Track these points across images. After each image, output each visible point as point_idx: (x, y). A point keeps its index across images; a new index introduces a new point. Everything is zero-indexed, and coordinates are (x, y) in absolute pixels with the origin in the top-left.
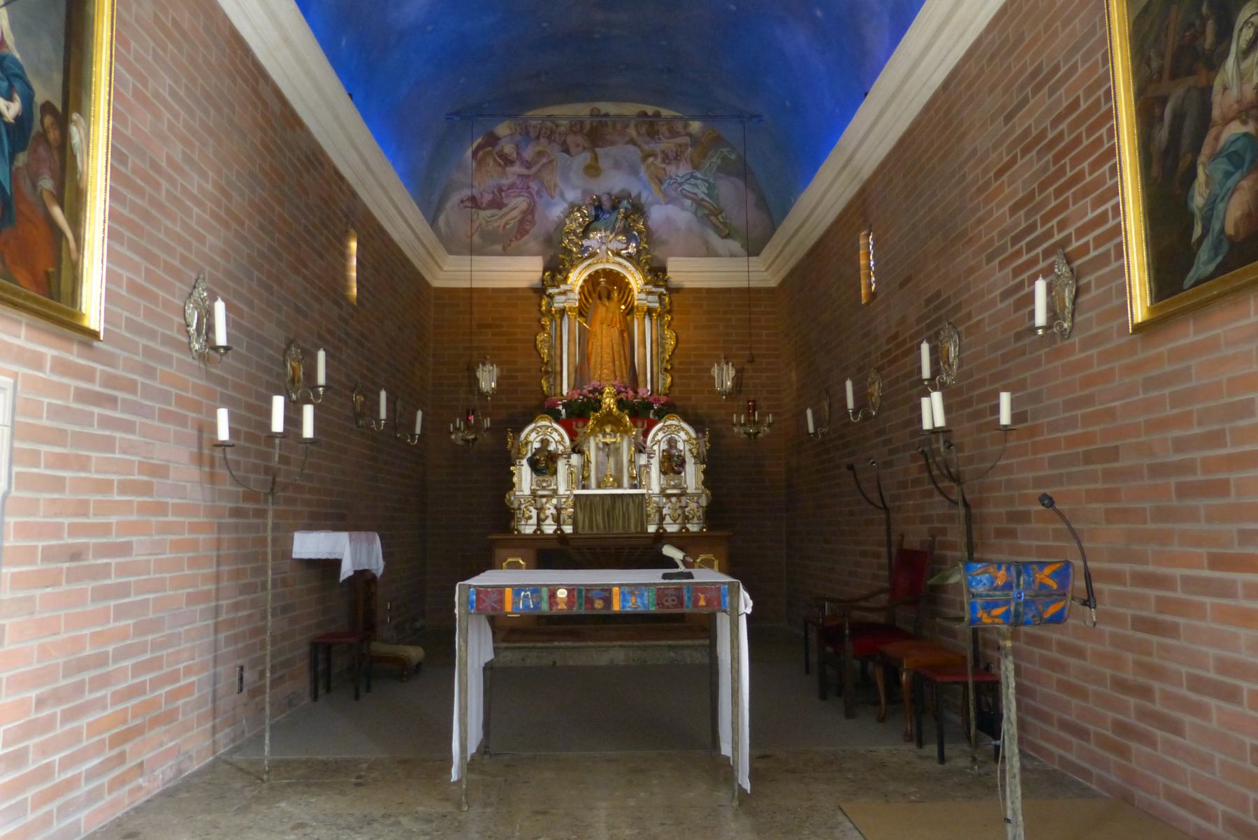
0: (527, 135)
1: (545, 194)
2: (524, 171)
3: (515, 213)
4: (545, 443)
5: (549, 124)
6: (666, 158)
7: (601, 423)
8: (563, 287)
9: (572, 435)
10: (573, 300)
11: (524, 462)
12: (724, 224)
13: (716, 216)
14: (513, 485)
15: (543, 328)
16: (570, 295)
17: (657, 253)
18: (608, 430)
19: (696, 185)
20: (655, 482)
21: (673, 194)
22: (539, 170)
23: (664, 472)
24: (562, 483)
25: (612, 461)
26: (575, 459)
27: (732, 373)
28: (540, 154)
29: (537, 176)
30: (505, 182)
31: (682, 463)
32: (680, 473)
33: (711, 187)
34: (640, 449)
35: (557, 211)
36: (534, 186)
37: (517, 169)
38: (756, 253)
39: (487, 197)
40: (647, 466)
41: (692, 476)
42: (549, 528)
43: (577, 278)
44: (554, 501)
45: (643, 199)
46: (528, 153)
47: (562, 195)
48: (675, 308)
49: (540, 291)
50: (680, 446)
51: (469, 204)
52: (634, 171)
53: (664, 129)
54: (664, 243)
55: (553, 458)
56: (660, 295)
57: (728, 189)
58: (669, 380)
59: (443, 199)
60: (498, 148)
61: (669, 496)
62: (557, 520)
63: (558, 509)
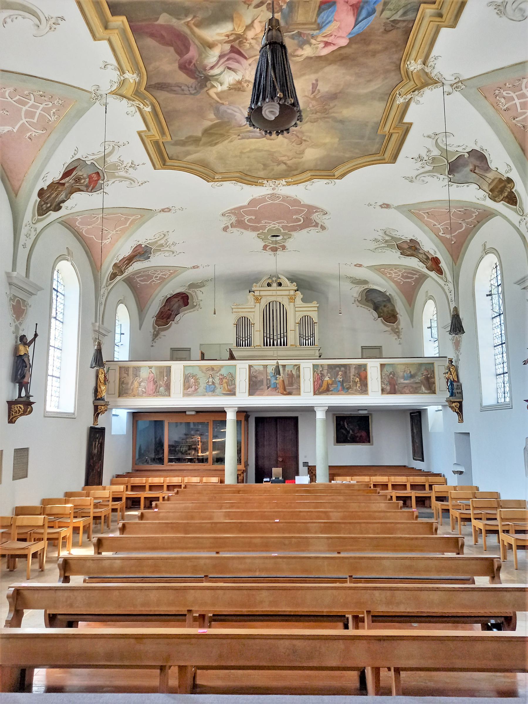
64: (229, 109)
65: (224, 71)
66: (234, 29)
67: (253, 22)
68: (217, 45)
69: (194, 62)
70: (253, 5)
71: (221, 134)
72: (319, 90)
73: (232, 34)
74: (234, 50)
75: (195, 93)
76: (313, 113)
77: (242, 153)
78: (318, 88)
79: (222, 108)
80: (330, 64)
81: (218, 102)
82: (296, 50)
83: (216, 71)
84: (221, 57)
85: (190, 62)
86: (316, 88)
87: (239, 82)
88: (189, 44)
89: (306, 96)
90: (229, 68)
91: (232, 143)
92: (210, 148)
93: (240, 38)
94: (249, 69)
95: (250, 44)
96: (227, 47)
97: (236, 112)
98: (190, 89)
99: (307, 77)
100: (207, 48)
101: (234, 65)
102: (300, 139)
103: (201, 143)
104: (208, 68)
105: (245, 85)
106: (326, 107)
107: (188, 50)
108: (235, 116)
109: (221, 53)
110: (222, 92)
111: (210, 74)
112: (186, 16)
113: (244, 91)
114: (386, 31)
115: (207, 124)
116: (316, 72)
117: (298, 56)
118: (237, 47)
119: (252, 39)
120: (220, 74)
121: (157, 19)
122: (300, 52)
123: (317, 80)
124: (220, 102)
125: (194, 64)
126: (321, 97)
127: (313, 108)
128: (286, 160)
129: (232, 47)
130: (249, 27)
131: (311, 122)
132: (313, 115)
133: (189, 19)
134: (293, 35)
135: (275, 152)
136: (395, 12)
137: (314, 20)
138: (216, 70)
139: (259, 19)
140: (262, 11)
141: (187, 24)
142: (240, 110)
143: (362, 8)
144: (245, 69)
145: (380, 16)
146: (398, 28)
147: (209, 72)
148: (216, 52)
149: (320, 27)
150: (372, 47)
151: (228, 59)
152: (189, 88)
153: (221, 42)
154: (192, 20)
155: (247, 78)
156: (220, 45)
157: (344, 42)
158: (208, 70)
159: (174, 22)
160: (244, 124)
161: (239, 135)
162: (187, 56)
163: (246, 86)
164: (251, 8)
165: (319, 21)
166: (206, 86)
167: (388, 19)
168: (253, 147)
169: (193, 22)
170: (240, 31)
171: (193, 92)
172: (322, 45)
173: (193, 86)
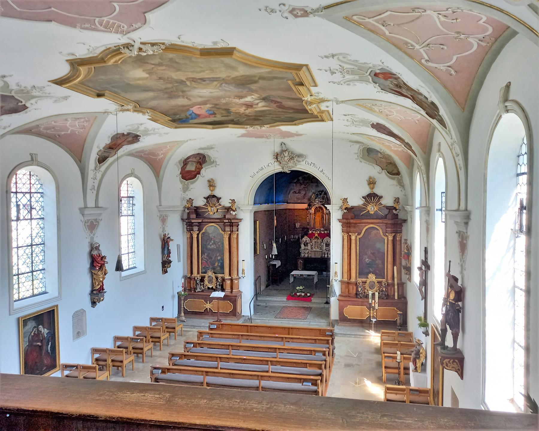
9: (311, 240)
29: (307, 187)
35: (310, 194)
36: (306, 189)
42: (306, 255)
49: (307, 209)
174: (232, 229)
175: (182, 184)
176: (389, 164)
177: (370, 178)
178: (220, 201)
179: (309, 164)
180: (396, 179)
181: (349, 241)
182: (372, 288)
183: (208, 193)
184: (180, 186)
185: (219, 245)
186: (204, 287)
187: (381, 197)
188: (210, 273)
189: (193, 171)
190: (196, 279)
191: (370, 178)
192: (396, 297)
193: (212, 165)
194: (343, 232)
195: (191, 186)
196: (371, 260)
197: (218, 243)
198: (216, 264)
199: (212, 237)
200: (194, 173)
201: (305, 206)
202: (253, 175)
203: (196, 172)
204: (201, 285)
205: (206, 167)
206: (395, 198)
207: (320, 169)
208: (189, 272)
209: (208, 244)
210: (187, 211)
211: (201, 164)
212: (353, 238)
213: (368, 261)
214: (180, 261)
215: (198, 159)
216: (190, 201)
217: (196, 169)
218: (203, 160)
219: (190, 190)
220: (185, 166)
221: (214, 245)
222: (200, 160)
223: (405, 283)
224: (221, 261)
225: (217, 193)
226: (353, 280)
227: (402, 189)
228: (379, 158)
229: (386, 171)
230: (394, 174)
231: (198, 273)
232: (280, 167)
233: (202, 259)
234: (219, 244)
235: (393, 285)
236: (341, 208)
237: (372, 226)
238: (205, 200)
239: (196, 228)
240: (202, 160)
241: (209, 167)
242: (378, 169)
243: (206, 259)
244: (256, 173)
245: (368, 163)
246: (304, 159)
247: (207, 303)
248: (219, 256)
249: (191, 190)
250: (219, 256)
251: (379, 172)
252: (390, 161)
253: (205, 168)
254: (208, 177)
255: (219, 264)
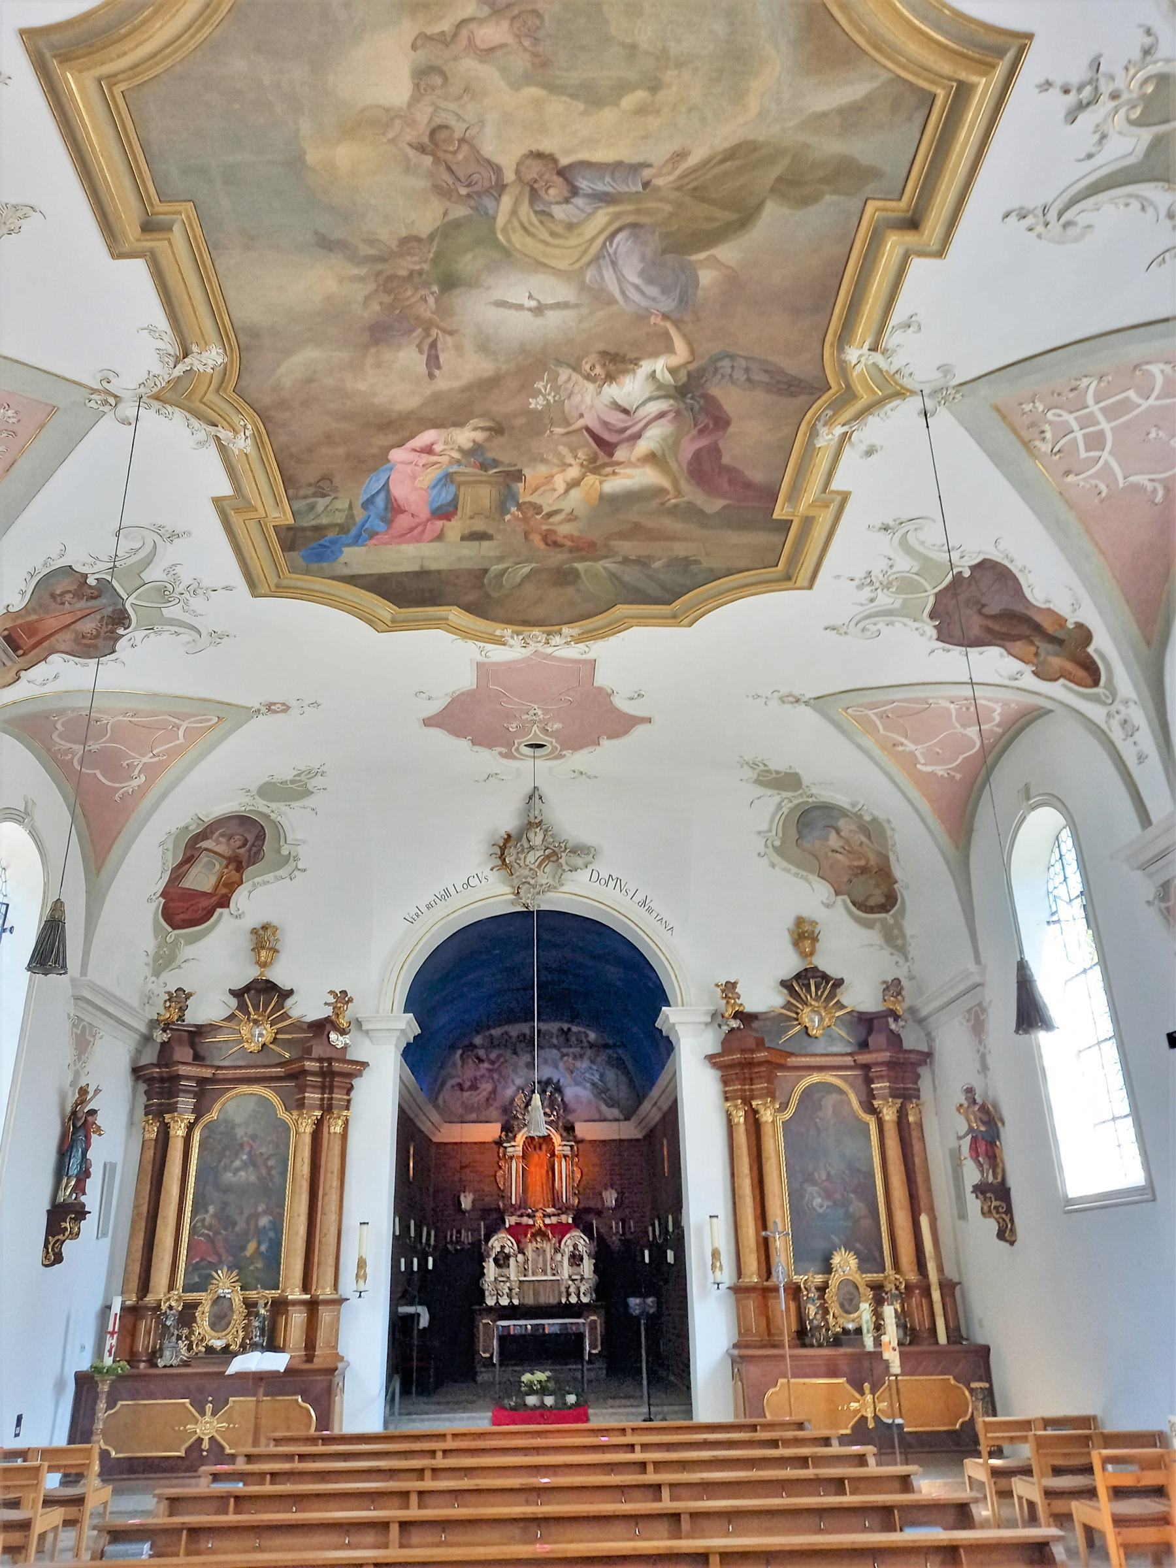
0: (492, 1044)
1: (502, 1080)
2: (490, 1066)
3: (484, 1093)
4: (503, 1247)
5: (506, 1037)
6: (575, 1058)
7: (534, 1235)
8: (513, 1144)
9: (518, 1242)
10: (519, 1151)
11: (491, 1260)
12: (610, 1098)
13: (605, 1093)
14: (484, 1274)
15: (500, 1167)
16: (517, 1148)
17: (570, 1118)
18: (539, 1239)
19: (593, 1074)
20: (566, 1270)
21: (580, 1080)
22: (500, 1066)
23: (571, 1265)
24: (513, 1272)
25: (541, 1259)
26: (520, 1257)
27: (615, 1195)
28: (499, 1056)
30: (478, 1074)
31: (581, 1259)
32: (579, 1265)
33: (602, 1076)
34: (557, 1250)
35: (510, 1092)
37: (486, 1065)
38: (627, 1119)
39: (467, 1084)
40: (561, 1262)
41: (587, 1266)
43: (520, 1138)
44: (508, 1284)
45: (561, 1084)
46: (493, 1056)
47: (513, 1082)
48: (580, 1153)
49: (499, 1143)
50: (580, 1248)
51: (456, 1088)
52: (556, 1067)
53: (573, 1039)
54: (574, 1111)
55: (507, 1257)
56: (571, 1146)
57: (611, 1075)
58: (577, 1201)
59: (443, 1085)
60: (475, 1052)
61: (573, 1280)
62: (510, 1296)
63: (510, 1289)
64: (654, 300)
65: (637, 408)
66: (601, 483)
67: (567, 491)
68: (638, 460)
69: (694, 432)
70: (564, 513)
71: (703, 200)
72: (421, 352)
73: (607, 475)
74: (607, 447)
75: (720, 359)
76: (420, 273)
77: (654, 86)
78: (425, 357)
79: (668, 304)
80: (412, 412)
81: (677, 324)
82: (488, 440)
83: (654, 407)
84: (638, 436)
85: (701, 432)
86: (428, 356)
87: (610, 378)
88: (690, 464)
89: (451, 333)
90: (626, 411)
91: (675, 146)
92: (761, 134)
93: (593, 466)
94: (583, 407)
95: (576, 457)
96: (620, 454)
97: (637, 287)
98: (729, 370)
99: (457, 384)
100: (659, 453)
101: (616, 419)
102: (441, 154)
103: (775, 172)
104: (672, 415)
105: (598, 370)
106: (387, 299)
107: (697, 457)
108: (642, 273)
109: (634, 444)
110: (655, 355)
111: (672, 402)
112: (676, 506)
113: (604, 354)
114: (327, 478)
115: (728, 252)
116: (437, 397)
117: (483, 429)
118: (601, 454)
119: (571, 465)
120: (650, 399)
121: (725, 507)
122: (480, 436)
123: (431, 376)
124: (669, 325)
125: (695, 425)
126: (410, 331)
127: (422, 292)
128: (481, 21)
129: (611, 455)
130: (574, 484)
131: (418, 239)
132: (417, 267)
133: (673, 501)
134: (495, 467)
135: (527, 79)
136: (330, 508)
137: (462, 488)
138: (654, 409)
139: (556, 494)
140: (550, 505)
141: (679, 493)
142: (623, 293)
143: (386, 508)
144: (592, 407)
145: (351, 502)
146: (310, 485)
147: (671, 405)
148: (644, 446)
149: (448, 478)
150: (341, 451)
151: (624, 430)
152: (731, 376)
153: (629, 464)
154: (669, 500)
155: (591, 387)
156: (633, 459)
157: (396, 455)
158: (670, 411)
159: (700, 499)
160: (620, 237)
161: (646, 185)
162: (704, 442)
163: (598, 367)
164: (568, 510)
165: (453, 489)
166: (689, 374)
167: (336, 498)
168: (608, 115)
169: (669, 497)
170: (591, 479)
171: (726, 363)
172: (438, 448)
173: (719, 376)
174: (331, 1099)
175: (156, 937)
176: (856, 875)
177: (800, 921)
178: (289, 1002)
179: (603, 882)
180: (878, 926)
181: (752, 1129)
182: (850, 1309)
183: (247, 974)
184: (149, 943)
185: (270, 1169)
186: (190, 1348)
187: (839, 983)
188: (225, 1284)
189: (204, 894)
190: (164, 1307)
191: (800, 921)
192: (942, 1338)
193: (280, 873)
194: (727, 1099)
195: (188, 951)
196: (830, 1203)
197: (268, 1159)
198: (251, 1247)
199: (245, 1139)
200: (205, 903)
201: (490, 1131)
202: (412, 913)
203: (213, 900)
204: (179, 1338)
205: (256, 880)
206: (885, 982)
207: (639, 897)
208: (134, 1284)
209: (226, 1168)
210: (160, 1036)
211: (240, 869)
212: (767, 1116)
213: (821, 1206)
214: (105, 1235)
215: (238, 843)
216: (179, 998)
217: (217, 887)
218: (254, 849)
219: (179, 967)
220: (187, 866)
221: (251, 1169)
222: (242, 851)
223: (959, 1283)
224: (271, 1234)
225: (280, 975)
226: (780, 1277)
227: (895, 958)
228: (830, 854)
229: (846, 897)
230: (871, 910)
231: (171, 1287)
232: (508, 890)
233: (193, 1230)
234: (271, 1163)
235: (927, 1292)
236: (716, 1017)
237: (816, 1078)
238: (233, 1002)
239: (185, 1103)
240: (250, 850)
241: (266, 878)
242: (823, 890)
243: (210, 1228)
244: (424, 909)
245: (794, 869)
246: (590, 858)
247: (203, 1414)
248: (265, 1212)
249: (183, 965)
250: (265, 1212)
251: (826, 901)
252: (862, 863)
253: (250, 882)
254: (253, 920)
255: (263, 1248)
